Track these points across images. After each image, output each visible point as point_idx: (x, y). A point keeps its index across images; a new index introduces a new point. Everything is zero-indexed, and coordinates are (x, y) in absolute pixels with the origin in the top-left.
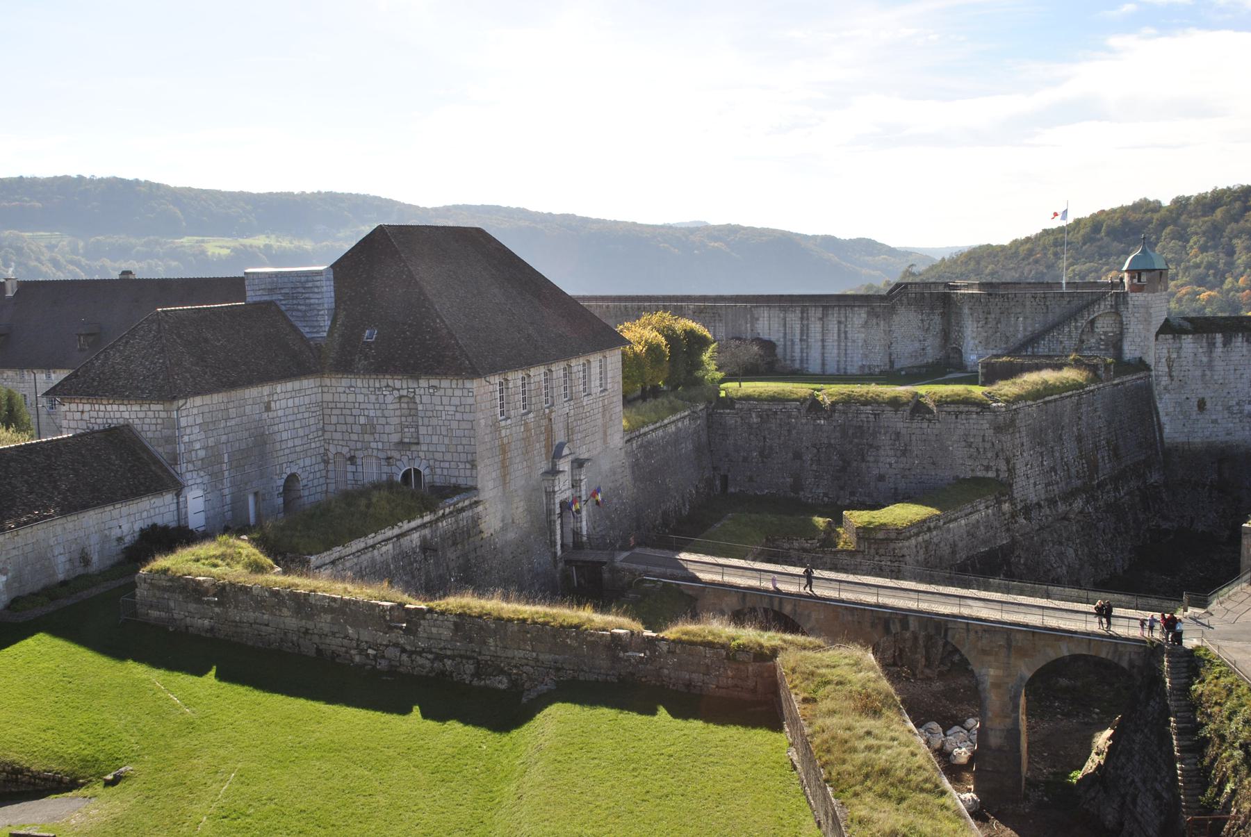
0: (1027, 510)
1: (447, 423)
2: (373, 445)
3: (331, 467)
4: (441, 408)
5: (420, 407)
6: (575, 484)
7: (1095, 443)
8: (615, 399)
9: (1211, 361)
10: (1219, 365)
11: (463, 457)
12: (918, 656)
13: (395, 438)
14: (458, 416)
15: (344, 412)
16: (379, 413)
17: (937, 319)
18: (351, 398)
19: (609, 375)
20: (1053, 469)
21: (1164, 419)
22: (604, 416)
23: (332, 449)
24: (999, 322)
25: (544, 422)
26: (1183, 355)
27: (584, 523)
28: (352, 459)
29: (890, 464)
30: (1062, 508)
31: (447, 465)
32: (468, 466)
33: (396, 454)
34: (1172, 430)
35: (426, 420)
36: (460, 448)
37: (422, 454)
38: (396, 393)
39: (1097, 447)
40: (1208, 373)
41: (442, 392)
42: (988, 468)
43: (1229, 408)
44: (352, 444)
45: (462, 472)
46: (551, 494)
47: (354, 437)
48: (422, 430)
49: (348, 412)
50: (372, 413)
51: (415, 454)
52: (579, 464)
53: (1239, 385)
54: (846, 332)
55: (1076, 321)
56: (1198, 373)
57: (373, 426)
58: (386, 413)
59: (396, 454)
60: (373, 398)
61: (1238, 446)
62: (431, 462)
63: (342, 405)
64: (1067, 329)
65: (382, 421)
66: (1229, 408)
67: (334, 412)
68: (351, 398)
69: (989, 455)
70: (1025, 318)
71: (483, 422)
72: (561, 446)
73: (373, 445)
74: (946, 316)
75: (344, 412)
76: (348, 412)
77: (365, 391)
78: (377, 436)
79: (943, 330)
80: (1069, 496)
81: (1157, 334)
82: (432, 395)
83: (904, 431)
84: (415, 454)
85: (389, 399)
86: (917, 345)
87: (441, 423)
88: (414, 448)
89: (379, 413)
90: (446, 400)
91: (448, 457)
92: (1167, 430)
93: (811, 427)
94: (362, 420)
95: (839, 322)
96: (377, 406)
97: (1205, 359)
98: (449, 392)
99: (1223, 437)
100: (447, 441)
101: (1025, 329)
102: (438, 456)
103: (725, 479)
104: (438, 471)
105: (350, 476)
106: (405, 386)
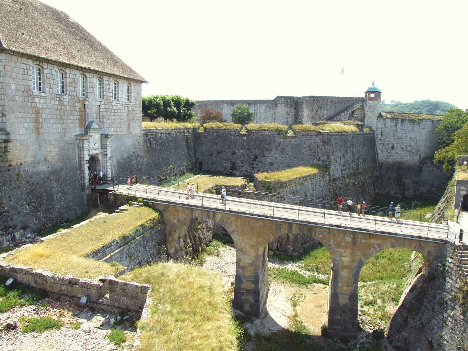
0: (335, 180)
6: (103, 146)
7: (358, 156)
8: (137, 109)
9: (396, 129)
10: (399, 131)
12: (289, 247)
17: (293, 110)
19: (133, 95)
20: (344, 165)
21: (379, 151)
22: (128, 115)
24: (317, 111)
25: (79, 105)
26: (387, 126)
27: (109, 170)
29: (276, 158)
30: (347, 181)
34: (382, 156)
39: (358, 158)
40: (395, 134)
42: (319, 160)
43: (402, 148)
46: (81, 149)
52: (105, 137)
53: (406, 139)
54: (257, 114)
55: (347, 111)
56: (392, 134)
61: (405, 163)
64: (343, 115)
66: (402, 148)
69: (320, 154)
70: (327, 110)
71: (13, 87)
72: (91, 123)
74: (296, 109)
79: (295, 115)
80: (349, 176)
81: (377, 118)
83: (282, 143)
86: (285, 120)
92: (380, 156)
93: (241, 140)
95: (255, 110)
97: (394, 128)
99: (399, 159)
101: (327, 114)
103: (201, 163)
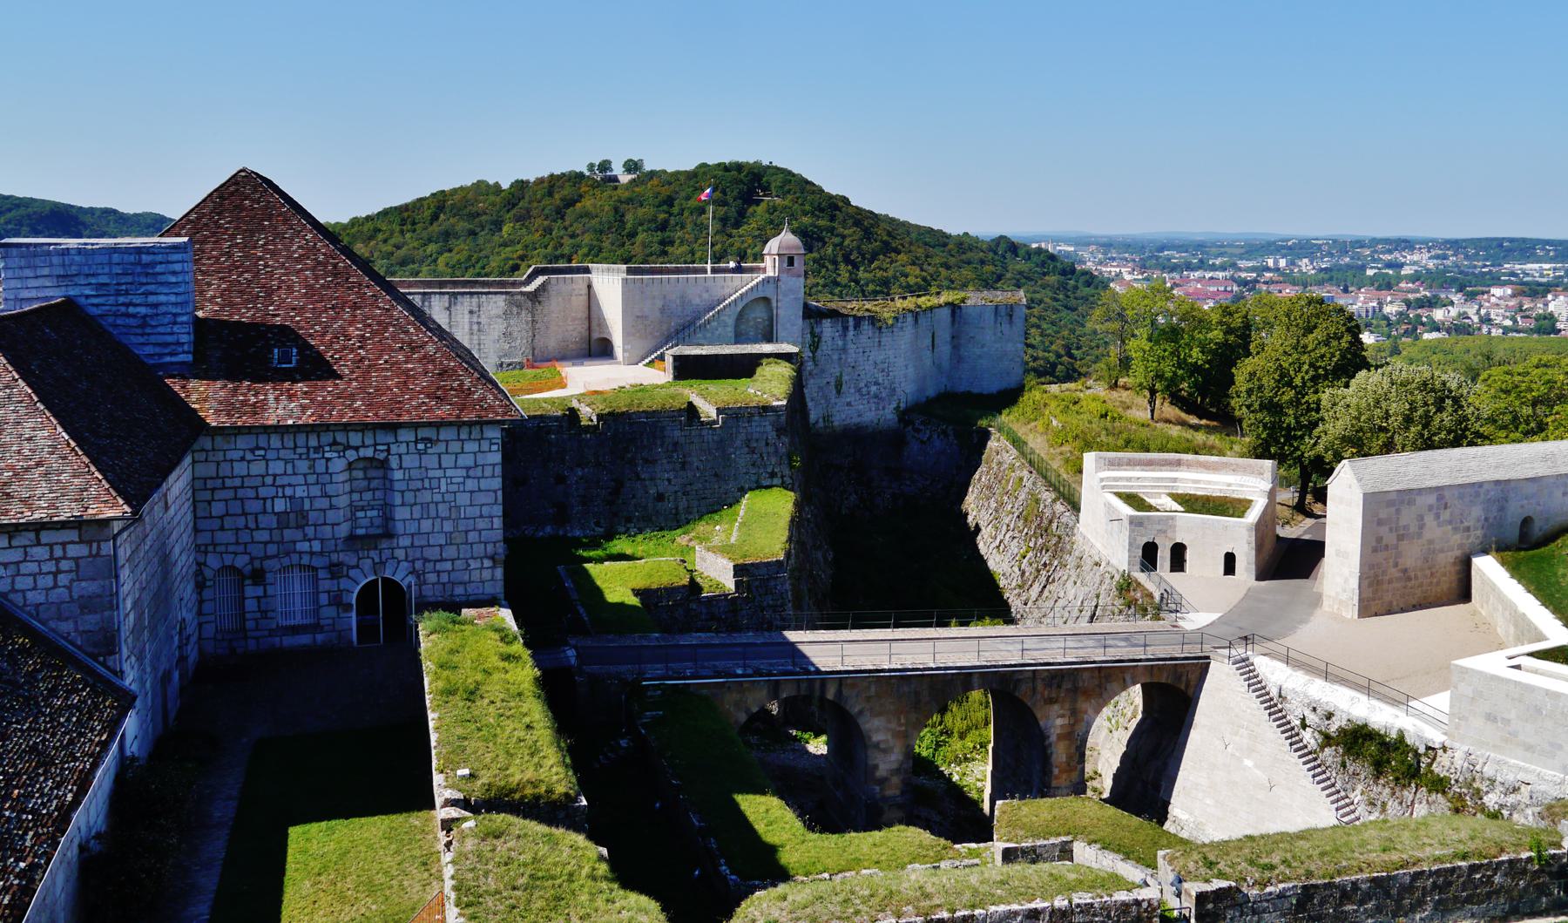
1: (448, 497)
2: (305, 546)
3: (207, 594)
4: (439, 473)
5: (398, 475)
11: (479, 549)
13: (343, 530)
14: (471, 485)
15: (241, 493)
16: (315, 491)
18: (258, 468)
23: (213, 562)
28: (258, 576)
31: (448, 566)
32: (487, 563)
33: (348, 558)
35: (409, 497)
36: (472, 536)
37: (400, 554)
38: (351, 455)
41: (441, 447)
44: (257, 551)
45: (476, 576)
47: (263, 536)
48: (401, 513)
49: (251, 493)
50: (300, 492)
51: (387, 553)
57: (302, 515)
58: (330, 489)
59: (348, 558)
60: (303, 466)
62: (418, 565)
63: (237, 482)
65: (324, 503)
67: (219, 495)
68: (258, 468)
73: (305, 546)
75: (241, 493)
76: (251, 493)
77: (288, 454)
78: (310, 531)
82: (420, 453)
84: (387, 553)
85: (338, 465)
87: (438, 498)
88: (384, 544)
89: (315, 491)
90: (447, 461)
91: (451, 552)
94: (280, 505)
96: (312, 479)
98: (455, 447)
100: (448, 526)
102: (429, 553)
104: (432, 578)
105: (250, 605)
106: (369, 441)
